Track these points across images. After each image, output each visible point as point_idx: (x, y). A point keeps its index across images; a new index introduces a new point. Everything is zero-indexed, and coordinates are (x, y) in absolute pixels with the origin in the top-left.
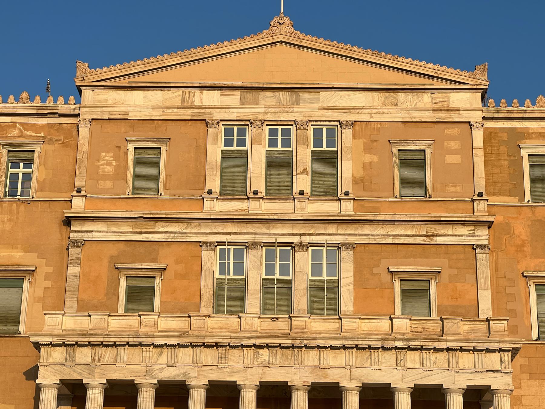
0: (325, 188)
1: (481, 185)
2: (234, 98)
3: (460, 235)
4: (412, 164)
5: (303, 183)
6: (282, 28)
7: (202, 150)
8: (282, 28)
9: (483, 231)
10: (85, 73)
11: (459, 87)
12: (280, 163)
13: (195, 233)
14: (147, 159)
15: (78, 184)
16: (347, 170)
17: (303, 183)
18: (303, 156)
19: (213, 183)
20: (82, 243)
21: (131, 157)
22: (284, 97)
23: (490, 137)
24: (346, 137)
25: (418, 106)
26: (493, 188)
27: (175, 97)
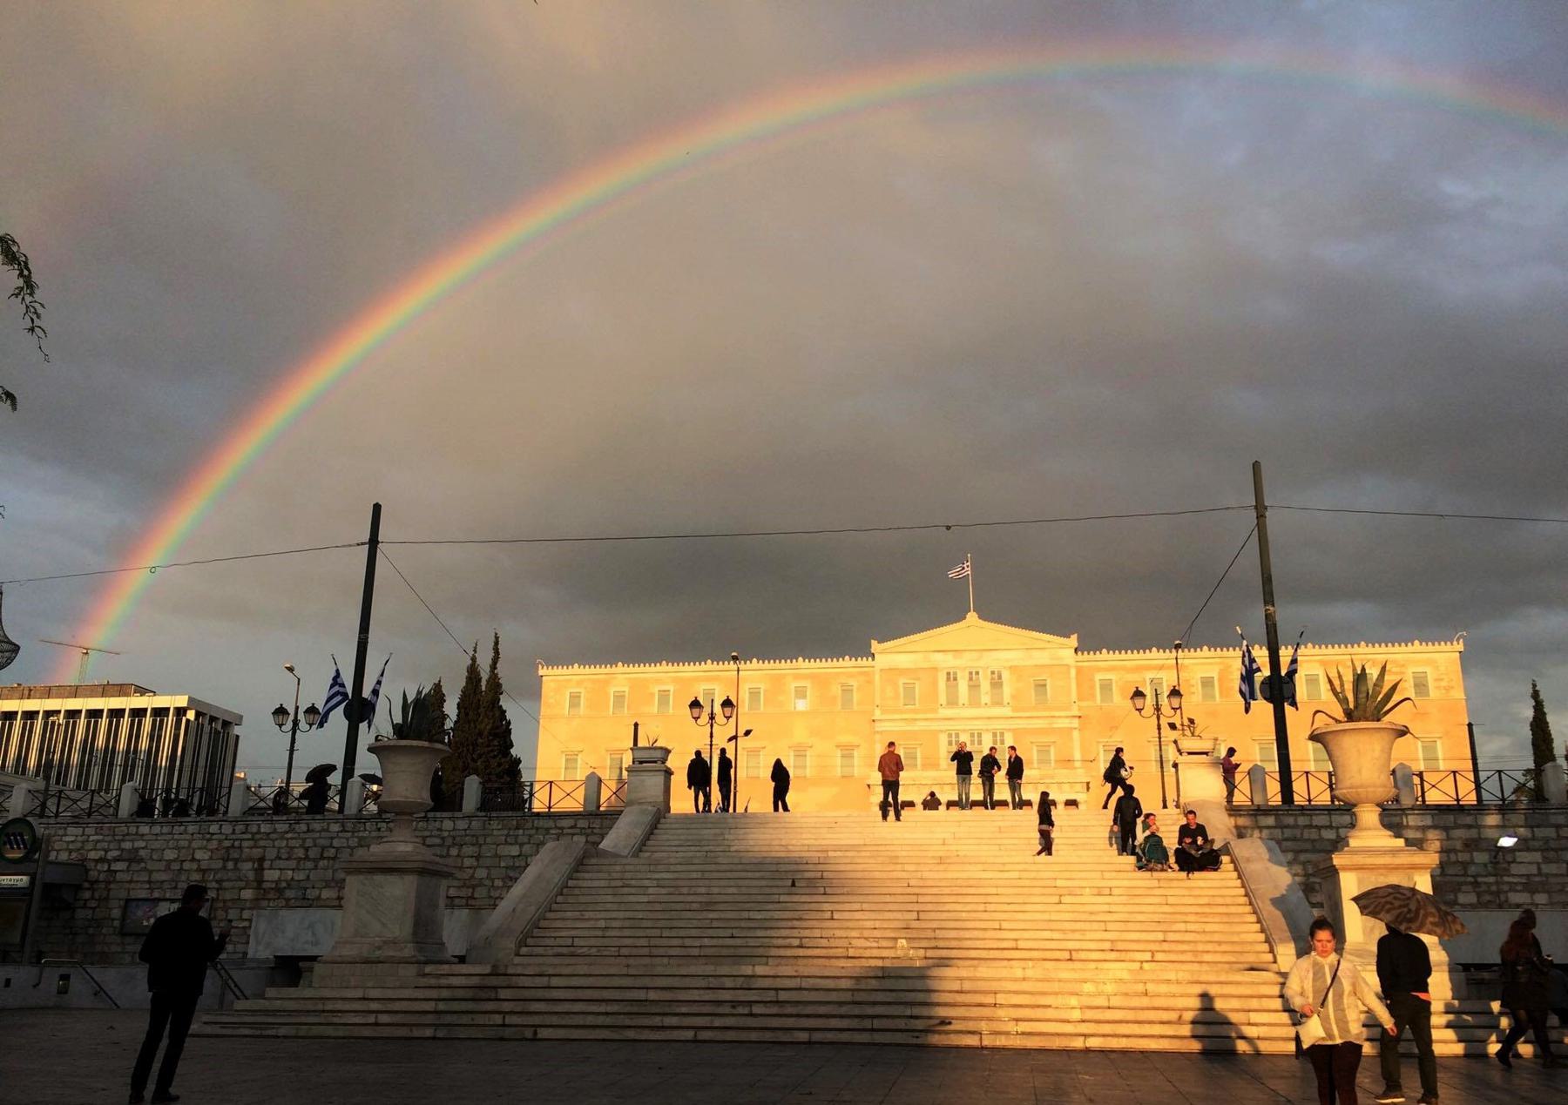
0: (998, 702)
1: (1074, 696)
2: (949, 656)
3: (1063, 723)
4: (1041, 686)
5: (985, 699)
6: (972, 617)
7: (935, 683)
8: (972, 617)
9: (1076, 721)
10: (875, 646)
11: (1062, 647)
12: (974, 686)
13: (935, 726)
14: (909, 690)
15: (878, 702)
16: (1007, 690)
17: (985, 699)
18: (985, 685)
19: (943, 699)
20: (881, 733)
21: (901, 690)
22: (974, 654)
23: (1079, 670)
24: (1006, 675)
25: (1042, 658)
26: (1081, 698)
27: (920, 656)
